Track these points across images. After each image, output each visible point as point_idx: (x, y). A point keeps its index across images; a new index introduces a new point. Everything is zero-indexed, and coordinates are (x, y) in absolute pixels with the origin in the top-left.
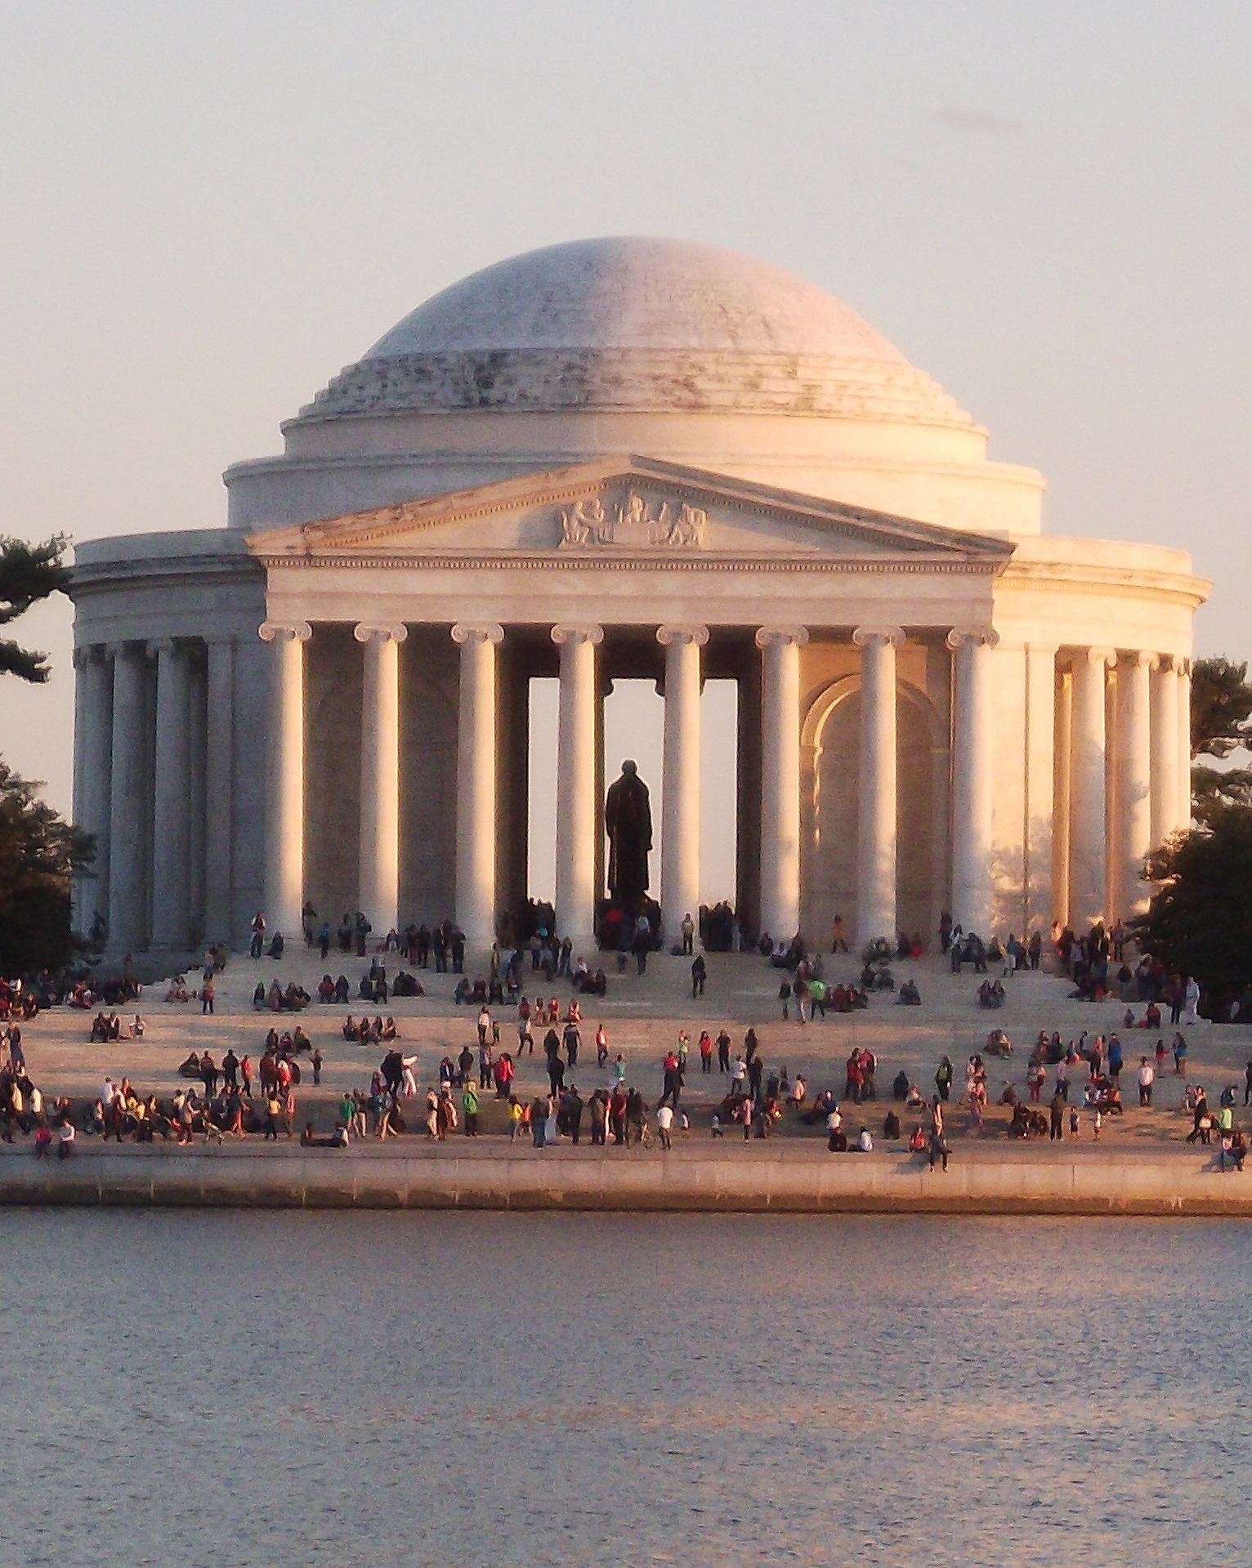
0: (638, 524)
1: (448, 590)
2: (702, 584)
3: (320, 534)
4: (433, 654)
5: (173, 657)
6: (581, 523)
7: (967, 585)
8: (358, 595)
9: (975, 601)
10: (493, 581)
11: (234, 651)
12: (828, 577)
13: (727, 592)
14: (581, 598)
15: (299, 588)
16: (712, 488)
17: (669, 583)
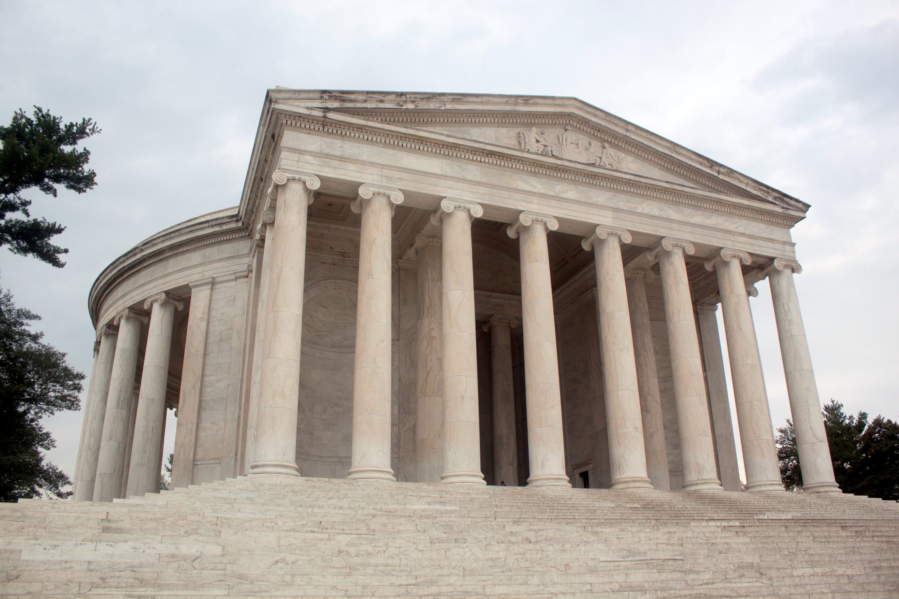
0: (576, 150)
1: (438, 171)
2: (623, 201)
3: (336, 105)
4: (416, 227)
5: (164, 304)
6: (538, 141)
7: (777, 233)
8: (364, 163)
9: (784, 243)
10: (473, 171)
11: (212, 289)
12: (699, 212)
13: (639, 210)
14: (542, 195)
15: (310, 148)
16: (628, 134)
17: (601, 196)
